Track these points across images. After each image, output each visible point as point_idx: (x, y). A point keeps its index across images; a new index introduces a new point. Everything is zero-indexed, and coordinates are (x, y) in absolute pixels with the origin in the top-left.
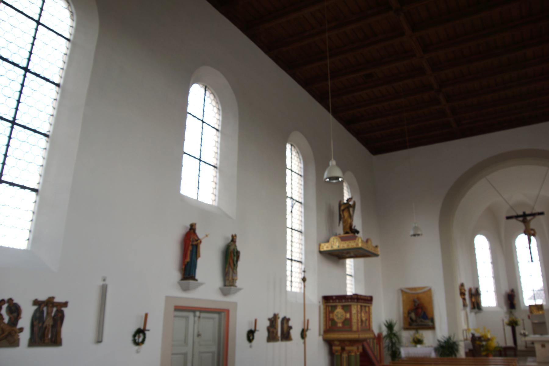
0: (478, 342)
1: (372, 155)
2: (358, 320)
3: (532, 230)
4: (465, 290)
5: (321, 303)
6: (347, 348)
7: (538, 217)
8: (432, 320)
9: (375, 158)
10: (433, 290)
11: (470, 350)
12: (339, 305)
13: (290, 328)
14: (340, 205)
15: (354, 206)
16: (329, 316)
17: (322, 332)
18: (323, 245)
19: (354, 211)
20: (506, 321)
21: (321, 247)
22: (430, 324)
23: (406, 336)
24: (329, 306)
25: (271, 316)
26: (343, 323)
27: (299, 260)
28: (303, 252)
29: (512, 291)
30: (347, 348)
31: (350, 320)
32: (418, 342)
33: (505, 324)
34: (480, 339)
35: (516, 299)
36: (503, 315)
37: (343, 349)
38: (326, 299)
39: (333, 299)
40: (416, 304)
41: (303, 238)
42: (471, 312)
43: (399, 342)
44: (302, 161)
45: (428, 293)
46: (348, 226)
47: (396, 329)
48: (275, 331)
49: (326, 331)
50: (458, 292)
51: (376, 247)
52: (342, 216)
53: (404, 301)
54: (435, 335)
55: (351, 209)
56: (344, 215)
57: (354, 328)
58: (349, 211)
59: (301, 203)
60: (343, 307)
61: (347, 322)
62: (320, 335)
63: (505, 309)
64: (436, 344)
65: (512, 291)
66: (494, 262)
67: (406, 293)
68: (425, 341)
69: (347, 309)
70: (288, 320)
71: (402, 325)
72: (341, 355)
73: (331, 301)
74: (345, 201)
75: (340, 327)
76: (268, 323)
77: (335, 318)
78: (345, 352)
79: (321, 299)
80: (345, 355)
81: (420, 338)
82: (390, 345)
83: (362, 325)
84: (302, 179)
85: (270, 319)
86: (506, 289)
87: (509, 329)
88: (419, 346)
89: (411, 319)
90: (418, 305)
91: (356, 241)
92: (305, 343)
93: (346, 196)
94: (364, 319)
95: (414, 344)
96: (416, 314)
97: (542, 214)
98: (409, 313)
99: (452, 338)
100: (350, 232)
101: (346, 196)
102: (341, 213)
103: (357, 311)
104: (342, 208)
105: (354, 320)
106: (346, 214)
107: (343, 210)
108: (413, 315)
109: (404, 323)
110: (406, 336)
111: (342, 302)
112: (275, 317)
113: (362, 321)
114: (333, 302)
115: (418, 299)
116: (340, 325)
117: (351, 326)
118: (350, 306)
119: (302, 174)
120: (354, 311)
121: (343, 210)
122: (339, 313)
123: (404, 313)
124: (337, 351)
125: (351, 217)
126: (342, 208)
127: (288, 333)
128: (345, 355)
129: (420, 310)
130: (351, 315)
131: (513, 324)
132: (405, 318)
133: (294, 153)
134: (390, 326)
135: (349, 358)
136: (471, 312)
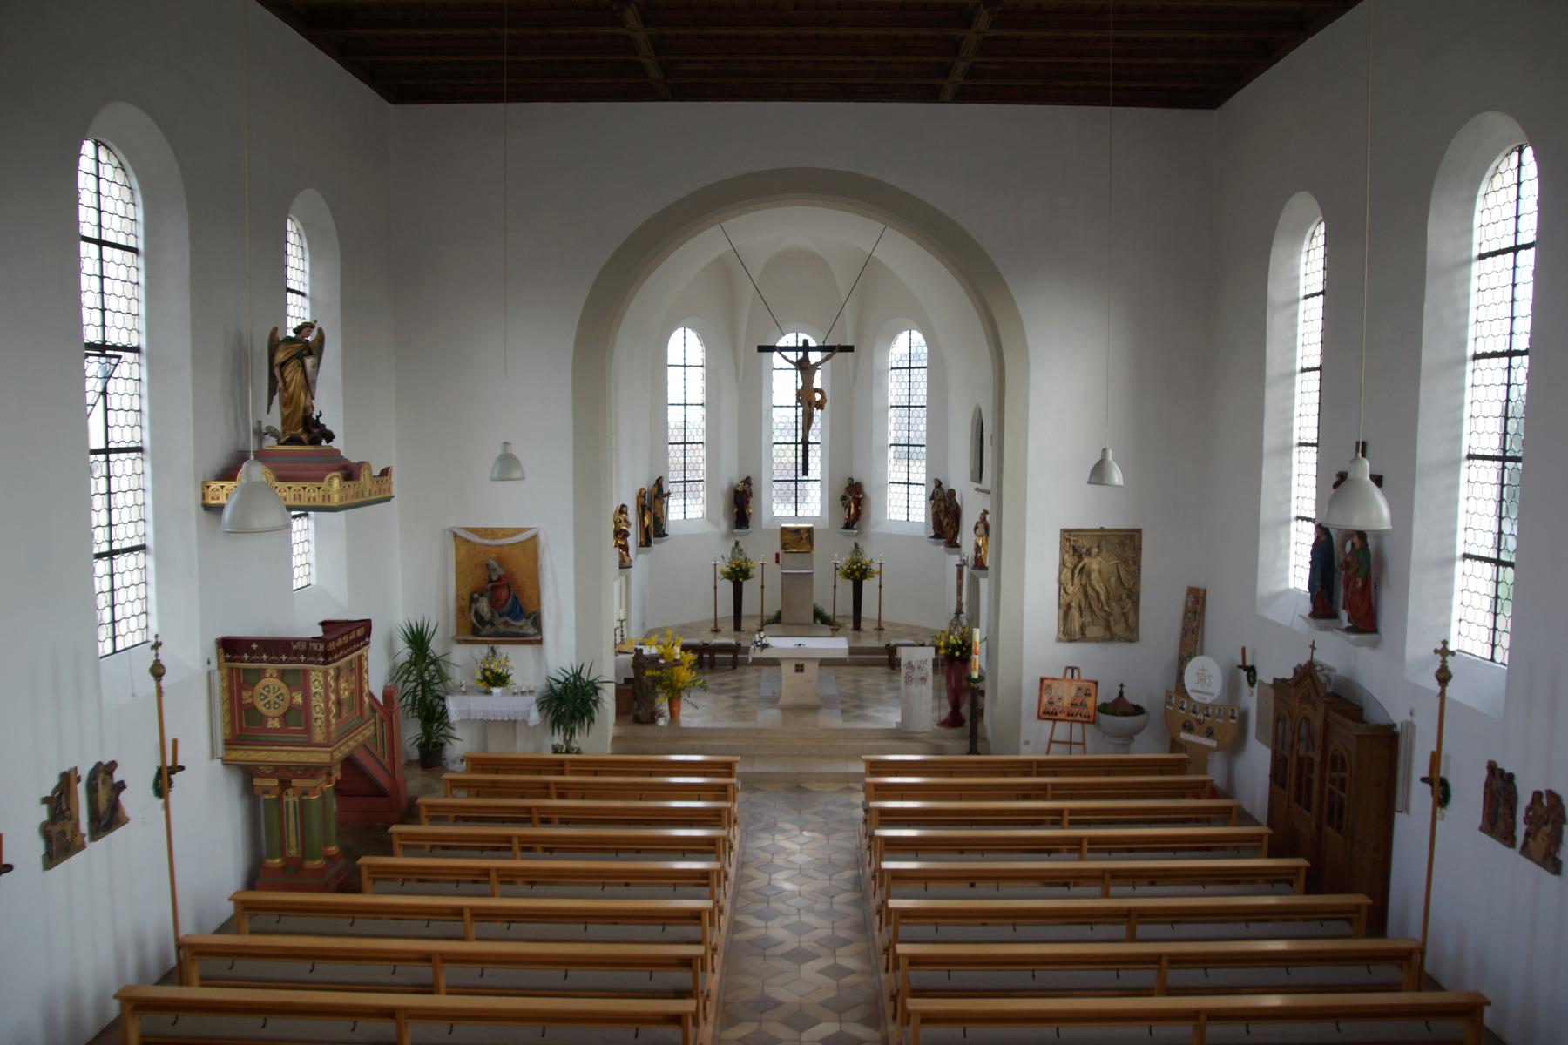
0: (649, 673)
1: (388, 104)
2: (327, 711)
3: (817, 390)
4: (628, 525)
5: (214, 665)
6: (295, 782)
7: (838, 355)
8: (537, 622)
9: (395, 110)
10: (542, 537)
11: (627, 681)
12: (272, 668)
13: (121, 786)
14: (274, 344)
15: (316, 349)
16: (240, 696)
17: (220, 751)
18: (215, 485)
19: (317, 366)
20: (724, 566)
21: (210, 493)
22: (531, 631)
23: (463, 659)
24: (238, 669)
25: (49, 785)
26: (284, 718)
27: (136, 542)
28: (150, 516)
29: (747, 481)
30: (295, 782)
31: (306, 706)
32: (495, 679)
33: (719, 575)
34: (653, 660)
35: (752, 500)
36: (719, 553)
37: (285, 785)
38: (230, 647)
39: (252, 652)
40: (495, 577)
41: (148, 468)
42: (638, 553)
43: (444, 679)
44: (139, 200)
45: (531, 548)
46: (300, 414)
47: (435, 647)
48: (69, 827)
49: (229, 744)
50: (610, 528)
51: (385, 472)
52: (280, 384)
53: (458, 564)
54: (540, 658)
55: (309, 361)
56: (285, 383)
57: (319, 735)
58: (303, 366)
59: (136, 350)
60: (282, 675)
61: (298, 716)
62: (213, 756)
63: (724, 526)
64: (539, 685)
65: (747, 481)
66: (711, 405)
67: (468, 541)
68: (515, 678)
69: (298, 681)
70: (112, 765)
71: (452, 631)
72: (280, 799)
73: (246, 657)
74: (291, 334)
75: (274, 730)
76: (43, 814)
77: (260, 705)
78: (290, 791)
79: (212, 651)
80: (291, 799)
81: (500, 670)
82: (419, 688)
83: (339, 715)
84: (141, 263)
85: (45, 800)
86: (731, 475)
87: (727, 587)
88: (496, 690)
89: (477, 613)
90: (499, 579)
91: (324, 485)
92: (167, 807)
93: (297, 312)
94: (345, 695)
95: (483, 686)
96: (493, 603)
97: (850, 349)
98: (472, 601)
99: (584, 675)
100: (304, 437)
101: (297, 312)
102: (277, 371)
103: (326, 686)
104: (281, 356)
105: (317, 714)
106: (293, 375)
107: (283, 365)
108: (484, 606)
109: (459, 625)
110: (463, 659)
111: (281, 662)
112: (67, 780)
113: (339, 703)
114: (252, 662)
115: (500, 560)
116: (275, 724)
117: (308, 729)
118: (305, 672)
119: (141, 247)
120: (316, 688)
121: (283, 365)
122: (271, 692)
123: (459, 597)
124: (267, 792)
125: (308, 386)
126: (281, 356)
127: (115, 806)
128: (291, 799)
129: (504, 593)
130: (307, 696)
131: (738, 575)
132: (461, 612)
133: (107, 172)
134: (418, 639)
135: (303, 806)
136: (638, 553)
